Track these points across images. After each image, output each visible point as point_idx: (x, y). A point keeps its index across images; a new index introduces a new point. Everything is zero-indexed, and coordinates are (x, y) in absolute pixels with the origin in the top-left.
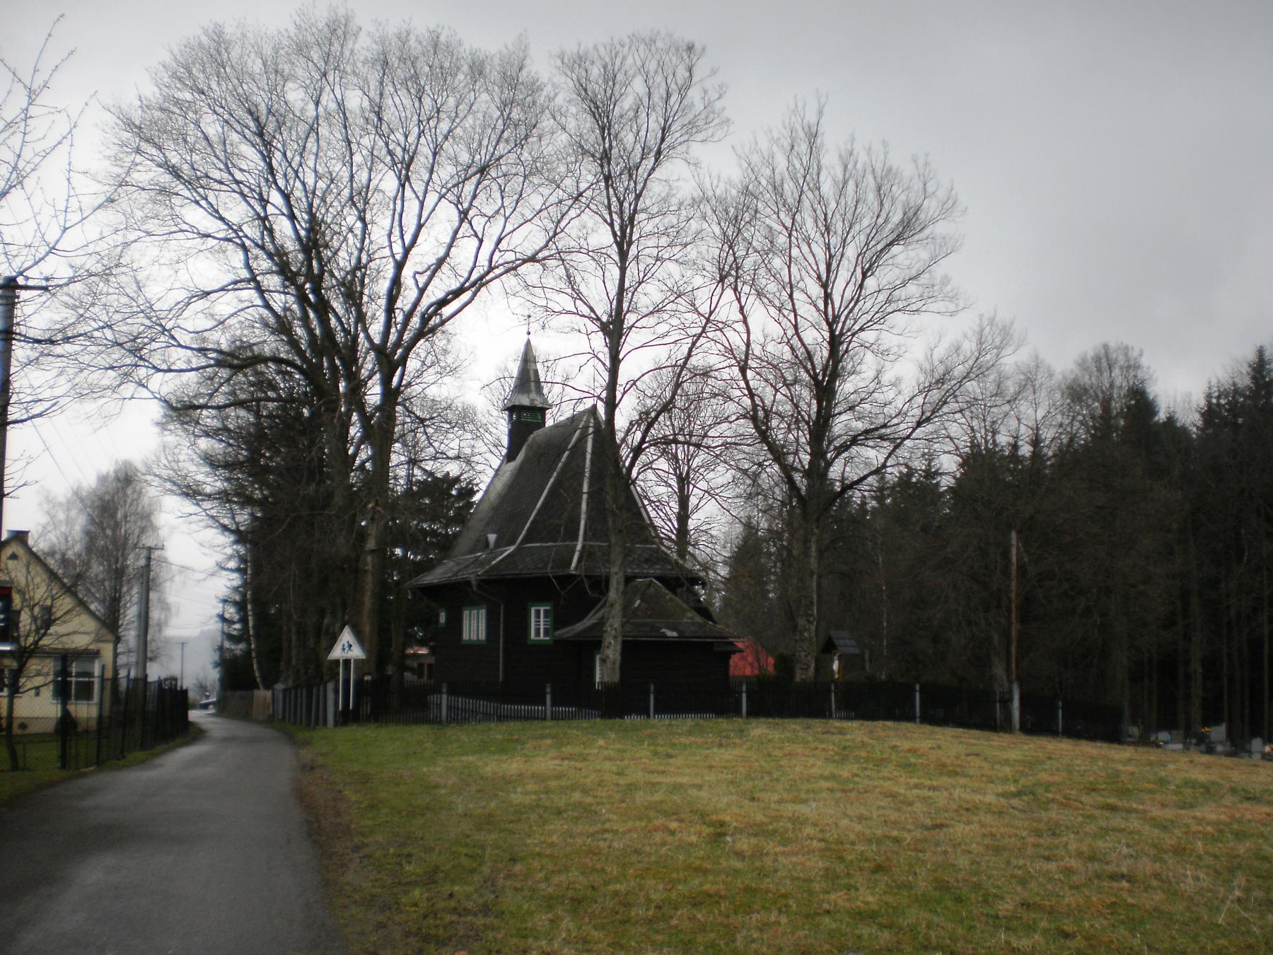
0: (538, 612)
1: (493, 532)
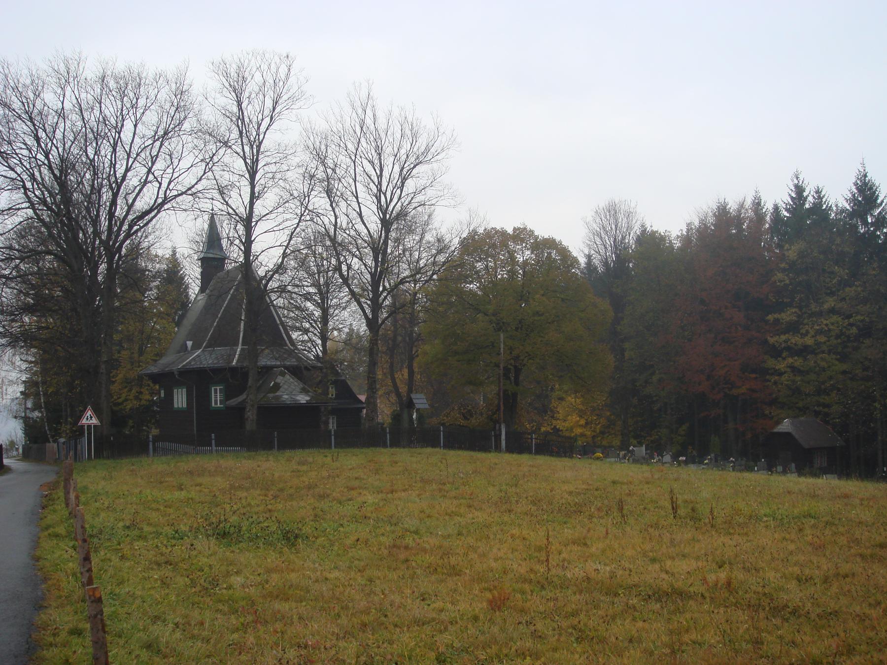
0: (216, 390)
1: (190, 340)
